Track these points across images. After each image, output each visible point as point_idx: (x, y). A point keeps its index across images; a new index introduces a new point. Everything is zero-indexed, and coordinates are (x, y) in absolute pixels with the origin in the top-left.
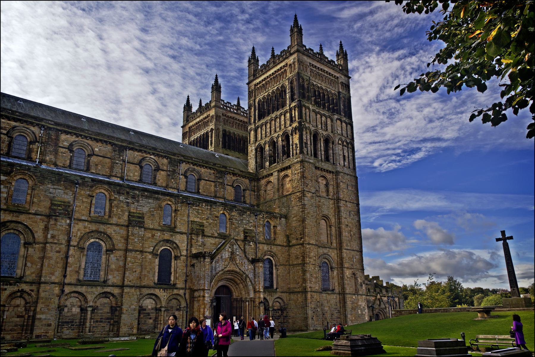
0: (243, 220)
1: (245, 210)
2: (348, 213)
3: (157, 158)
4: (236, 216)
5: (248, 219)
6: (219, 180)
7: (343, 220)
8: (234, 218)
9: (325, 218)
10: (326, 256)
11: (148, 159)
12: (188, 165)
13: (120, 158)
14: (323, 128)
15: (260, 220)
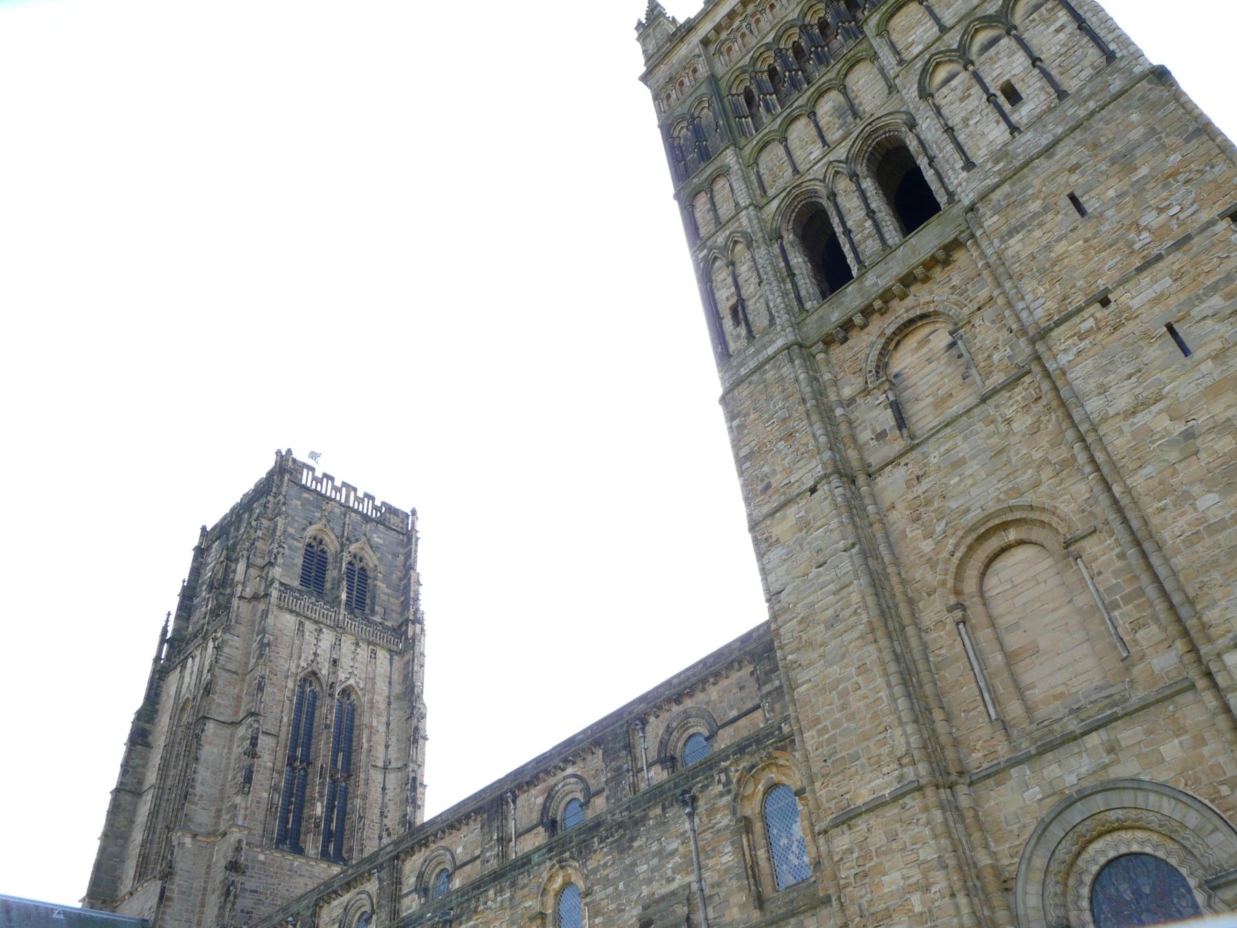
0: (634, 864)
1: (638, 814)
2: (1160, 351)
3: (581, 764)
4: (605, 866)
5: (655, 847)
6: (767, 688)
7: (1119, 441)
8: (598, 882)
9: (1012, 535)
10: (1099, 802)
11: (560, 786)
12: (665, 716)
13: (491, 839)
14: (833, 136)
15: (712, 812)
